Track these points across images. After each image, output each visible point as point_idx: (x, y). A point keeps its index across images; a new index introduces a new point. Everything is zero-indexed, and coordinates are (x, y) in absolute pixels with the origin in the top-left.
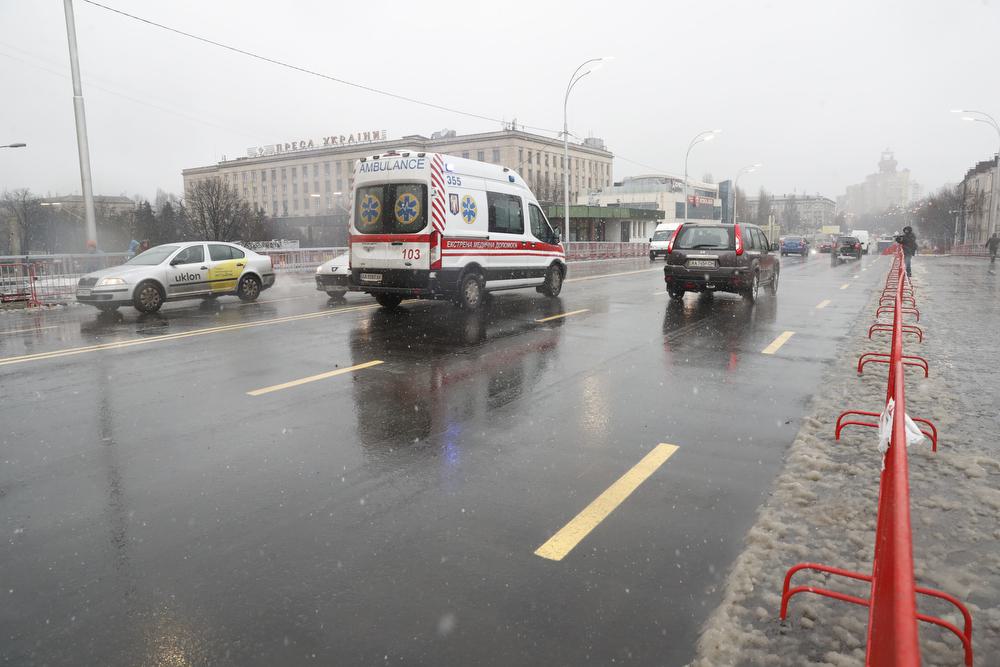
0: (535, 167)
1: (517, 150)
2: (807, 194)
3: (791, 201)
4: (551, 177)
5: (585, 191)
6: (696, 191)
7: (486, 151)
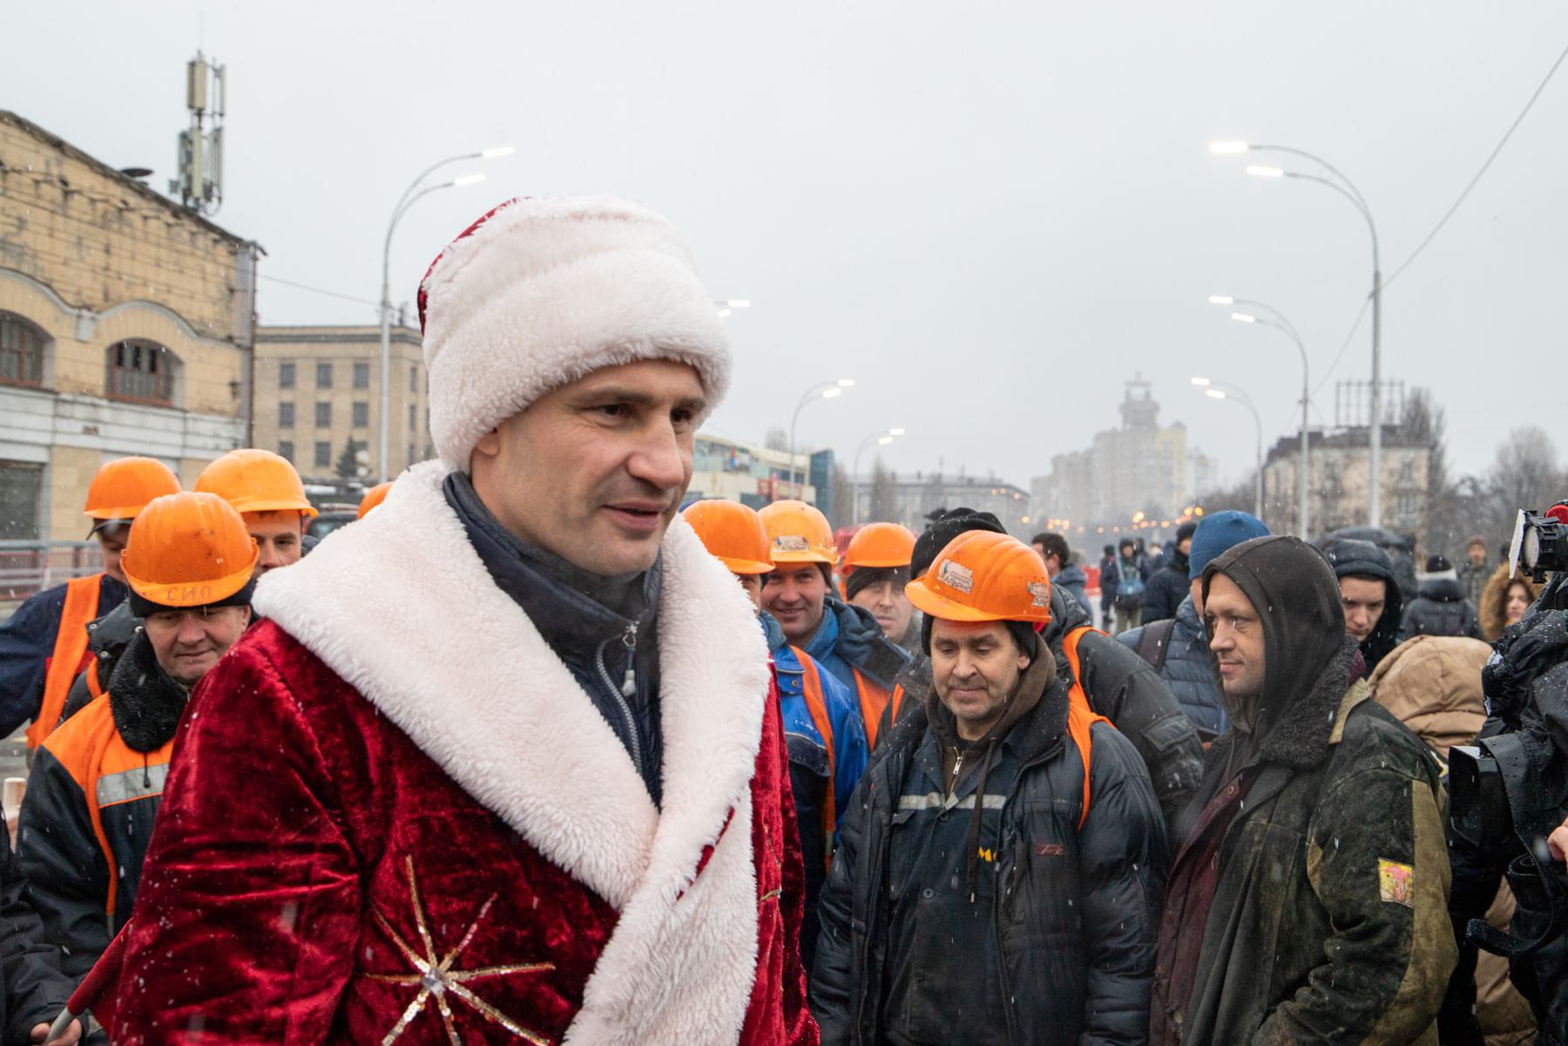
1: (407, 366)
2: (969, 473)
6: (772, 470)
7: (336, 363)
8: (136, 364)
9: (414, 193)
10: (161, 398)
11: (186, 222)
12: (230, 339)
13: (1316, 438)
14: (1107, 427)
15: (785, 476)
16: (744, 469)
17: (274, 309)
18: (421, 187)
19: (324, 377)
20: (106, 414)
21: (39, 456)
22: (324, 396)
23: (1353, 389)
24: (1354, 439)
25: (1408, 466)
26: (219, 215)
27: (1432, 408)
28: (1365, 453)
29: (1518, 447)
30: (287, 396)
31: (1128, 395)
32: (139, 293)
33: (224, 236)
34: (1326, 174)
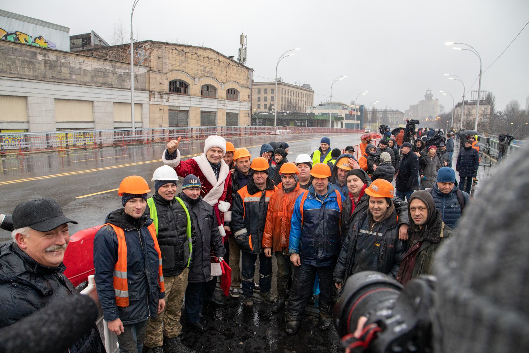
0: (287, 96)
1: (281, 89)
2: (392, 109)
3: (385, 112)
4: (292, 100)
5: (309, 107)
6: (352, 109)
7: (268, 89)
8: (232, 93)
9: (281, 58)
10: (236, 99)
11: (240, 66)
12: (248, 87)
13: (466, 103)
14: (421, 100)
15: (354, 110)
16: (346, 109)
17: (257, 79)
18: (283, 56)
19: (266, 92)
20: (226, 102)
21: (215, 110)
22: (266, 95)
23: (475, 92)
24: (474, 103)
25: (486, 109)
26: (246, 64)
27: (492, 97)
28: (476, 106)
29: (511, 105)
30: (259, 96)
31: (426, 93)
32: (232, 79)
33: (247, 68)
34: (471, 49)
